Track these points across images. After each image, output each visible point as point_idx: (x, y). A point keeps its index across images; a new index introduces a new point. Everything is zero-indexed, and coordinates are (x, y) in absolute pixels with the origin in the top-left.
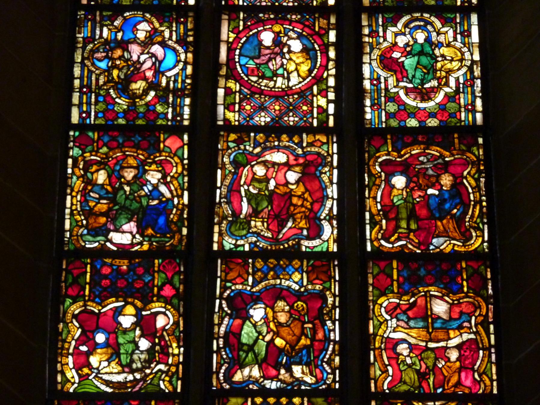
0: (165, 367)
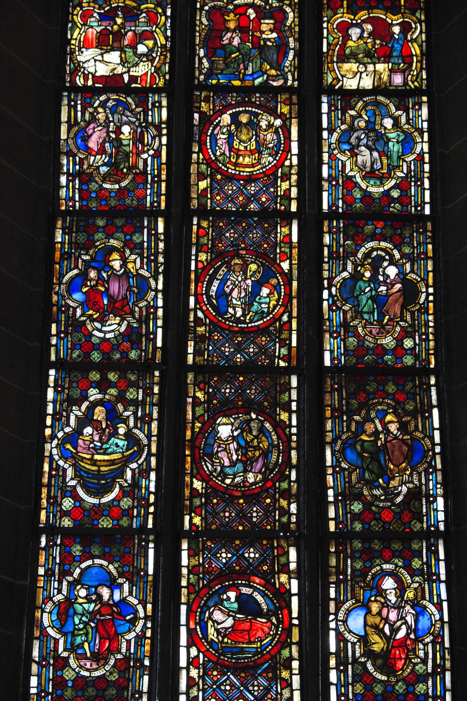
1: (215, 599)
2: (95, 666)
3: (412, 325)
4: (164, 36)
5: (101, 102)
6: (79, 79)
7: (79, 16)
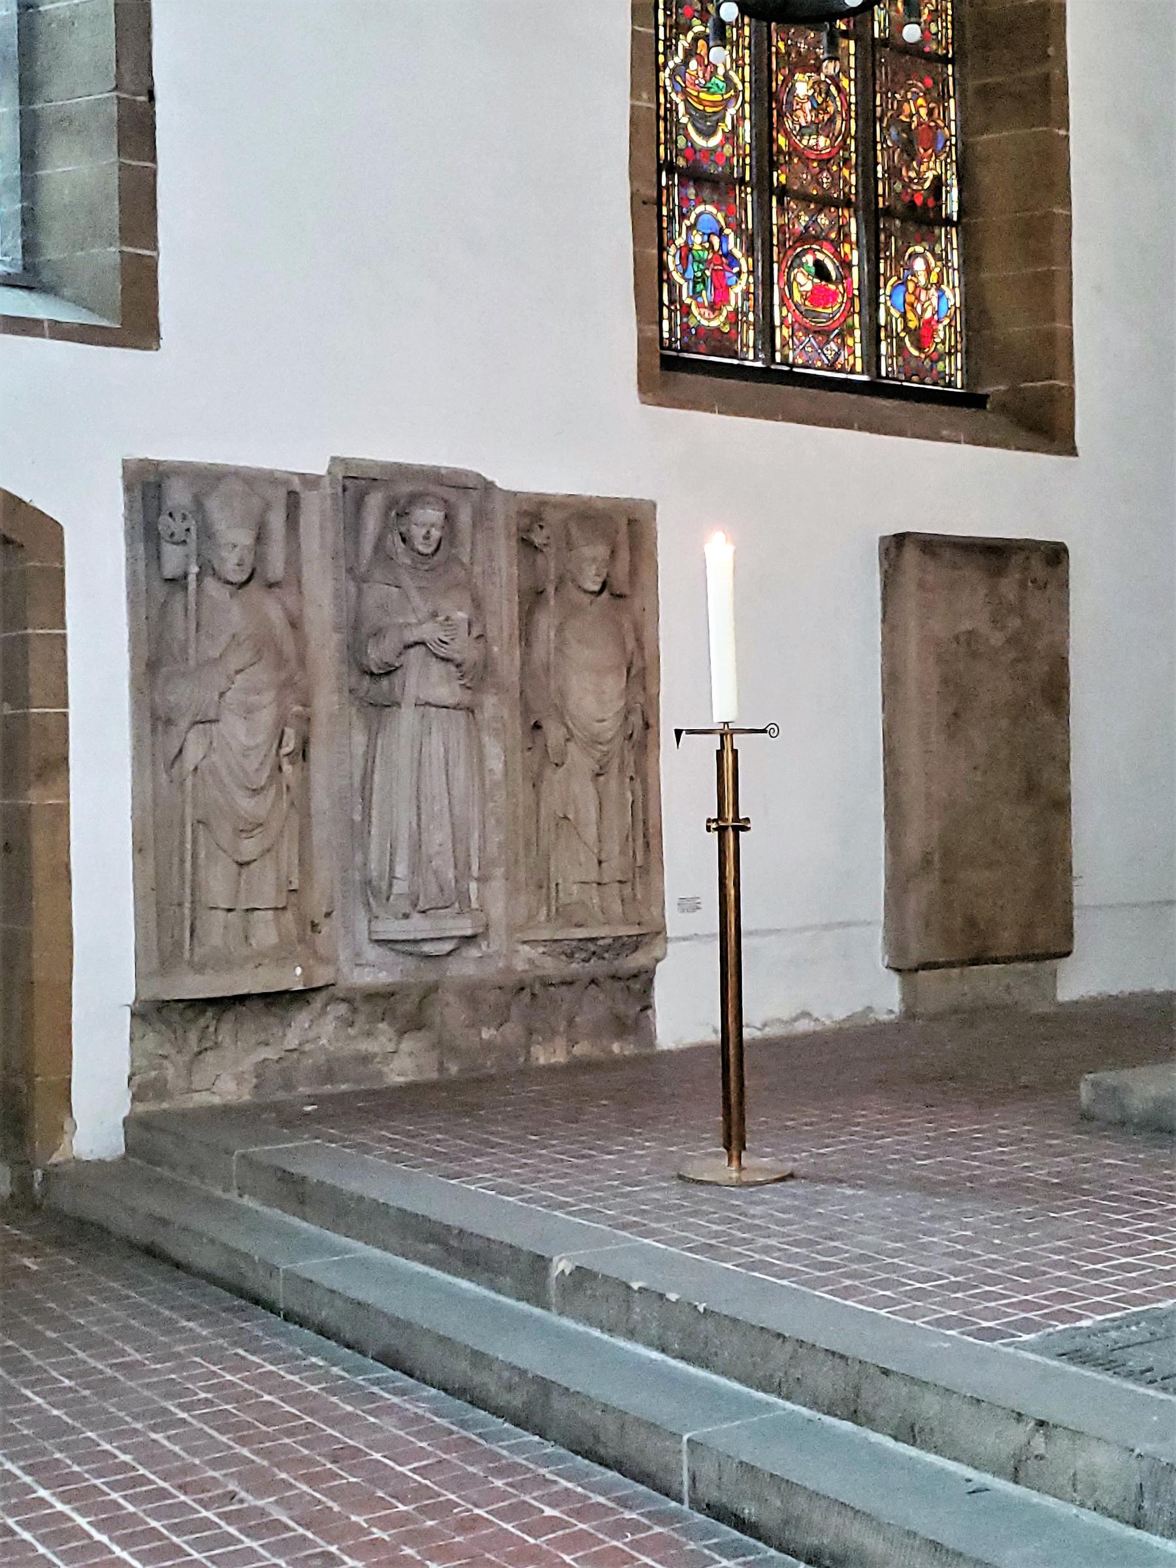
1: (798, 261)
2: (712, 316)
3: (936, 10)
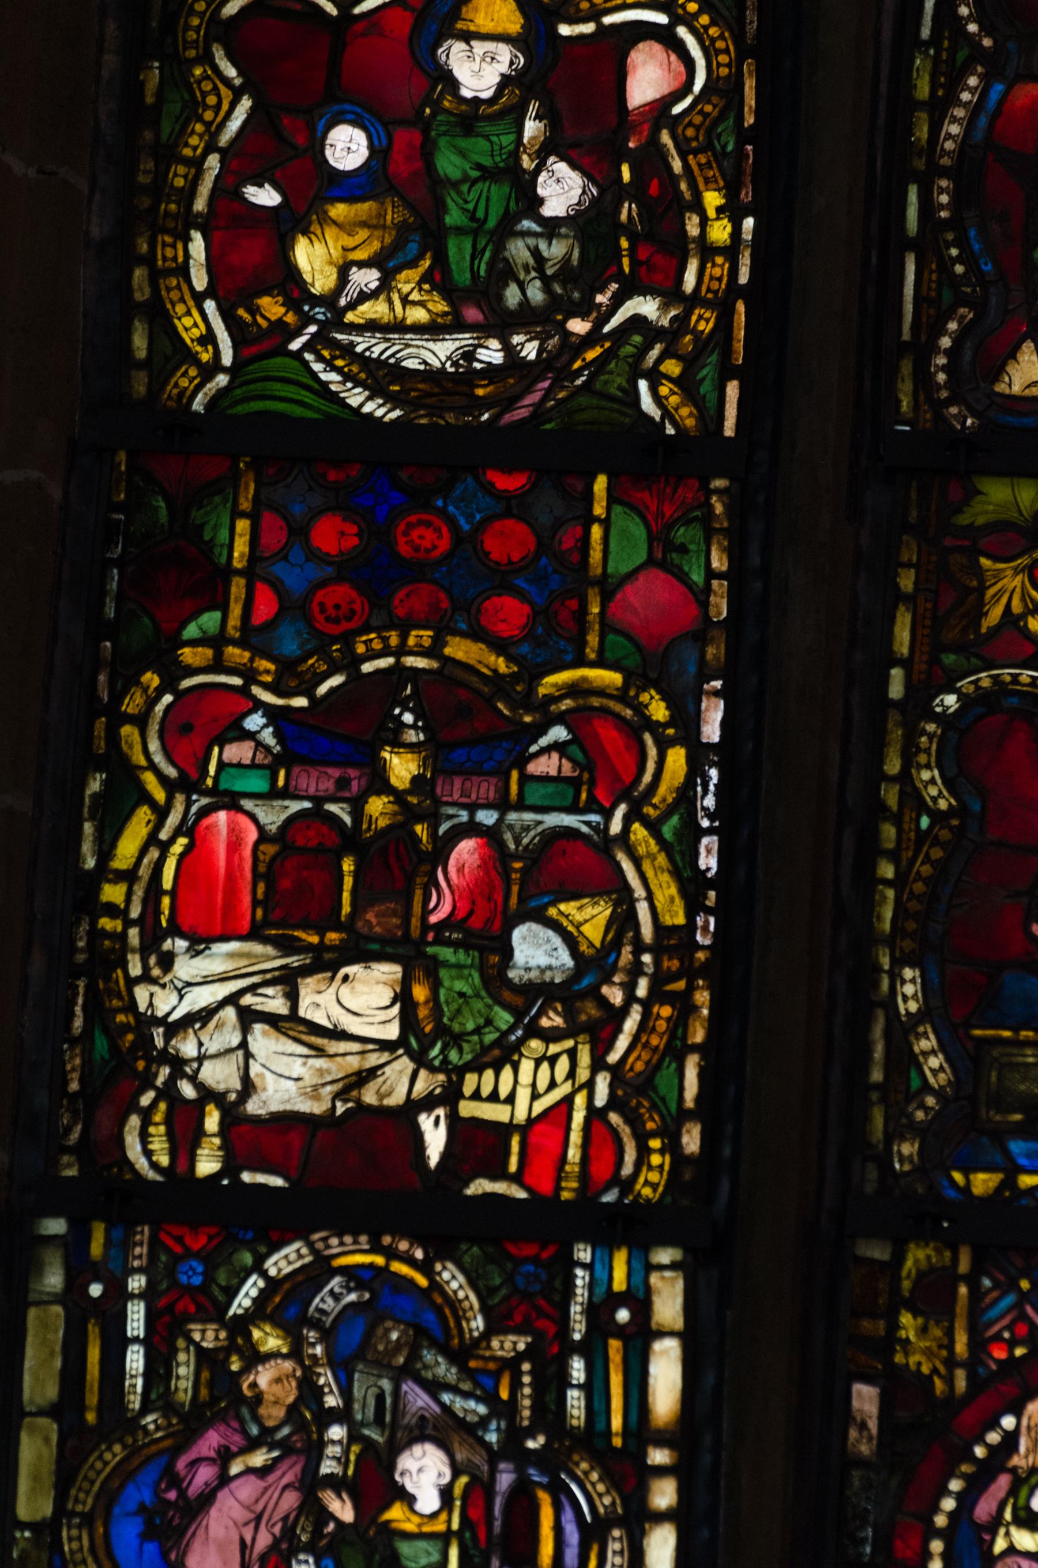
0: (664, 307)
4: (676, 873)
5: (273, 1284)
6: (144, 1136)
7: (154, 728)
